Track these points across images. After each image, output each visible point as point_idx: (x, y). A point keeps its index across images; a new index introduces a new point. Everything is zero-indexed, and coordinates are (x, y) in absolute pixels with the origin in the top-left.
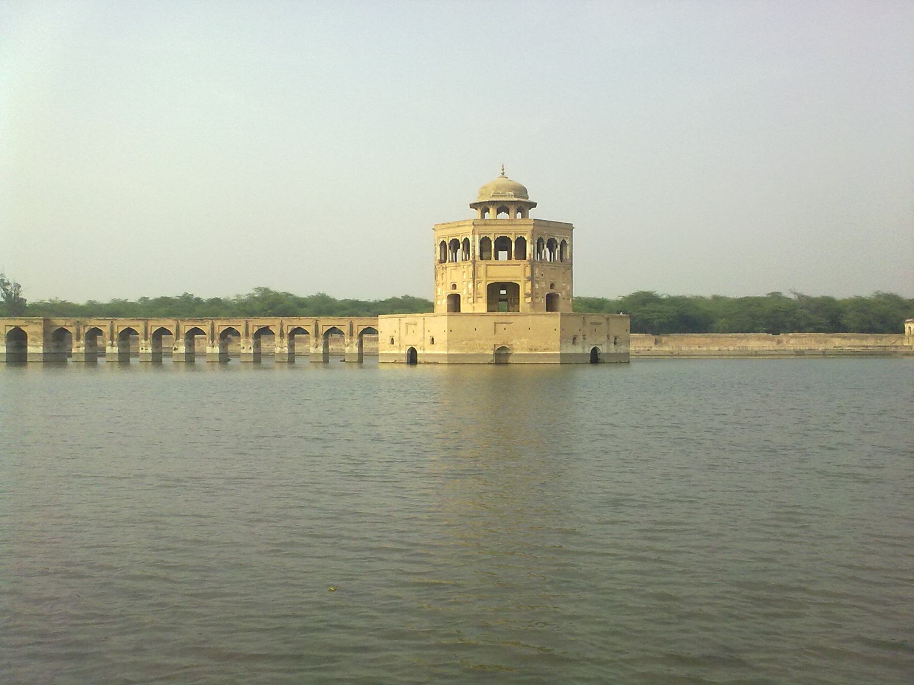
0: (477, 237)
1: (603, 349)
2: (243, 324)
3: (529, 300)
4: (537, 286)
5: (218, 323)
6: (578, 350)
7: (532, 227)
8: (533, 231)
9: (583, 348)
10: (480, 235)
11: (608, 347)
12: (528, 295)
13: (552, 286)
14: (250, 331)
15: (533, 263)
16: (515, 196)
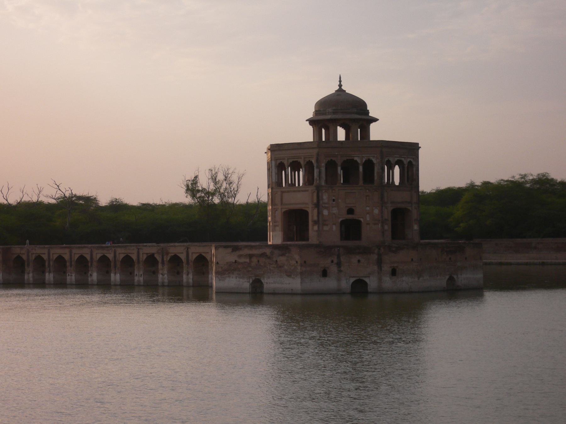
0: (273, 162)
1: (372, 283)
2: (135, 251)
3: (316, 228)
4: (326, 212)
5: (119, 251)
6: (330, 283)
7: (316, 151)
8: (318, 155)
9: (339, 280)
10: (276, 160)
11: (380, 280)
12: (316, 222)
13: (350, 211)
14: (141, 260)
15: (318, 189)
16: (335, 113)
